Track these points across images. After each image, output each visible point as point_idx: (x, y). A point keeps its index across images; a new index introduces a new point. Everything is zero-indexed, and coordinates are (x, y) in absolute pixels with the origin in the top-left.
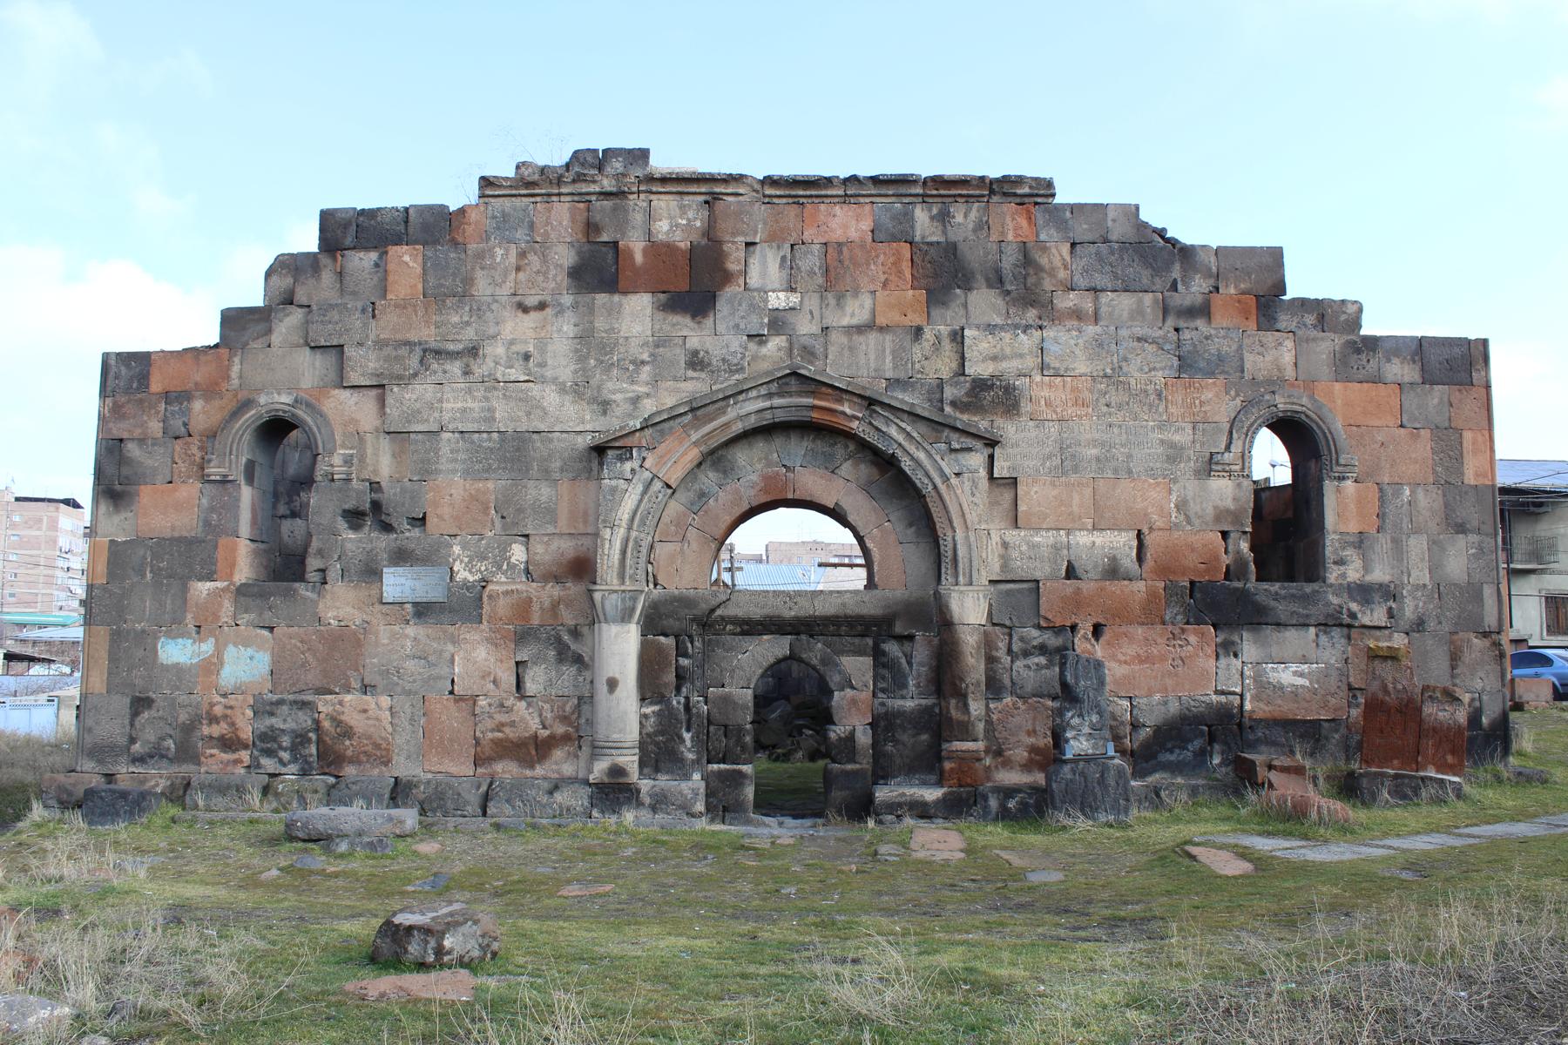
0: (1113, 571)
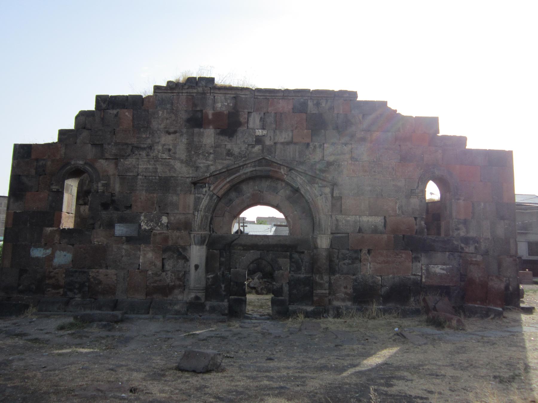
0: (375, 230)
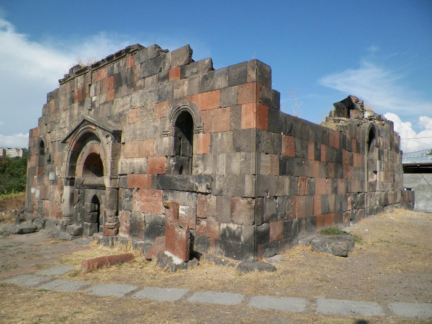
0: (141, 172)
